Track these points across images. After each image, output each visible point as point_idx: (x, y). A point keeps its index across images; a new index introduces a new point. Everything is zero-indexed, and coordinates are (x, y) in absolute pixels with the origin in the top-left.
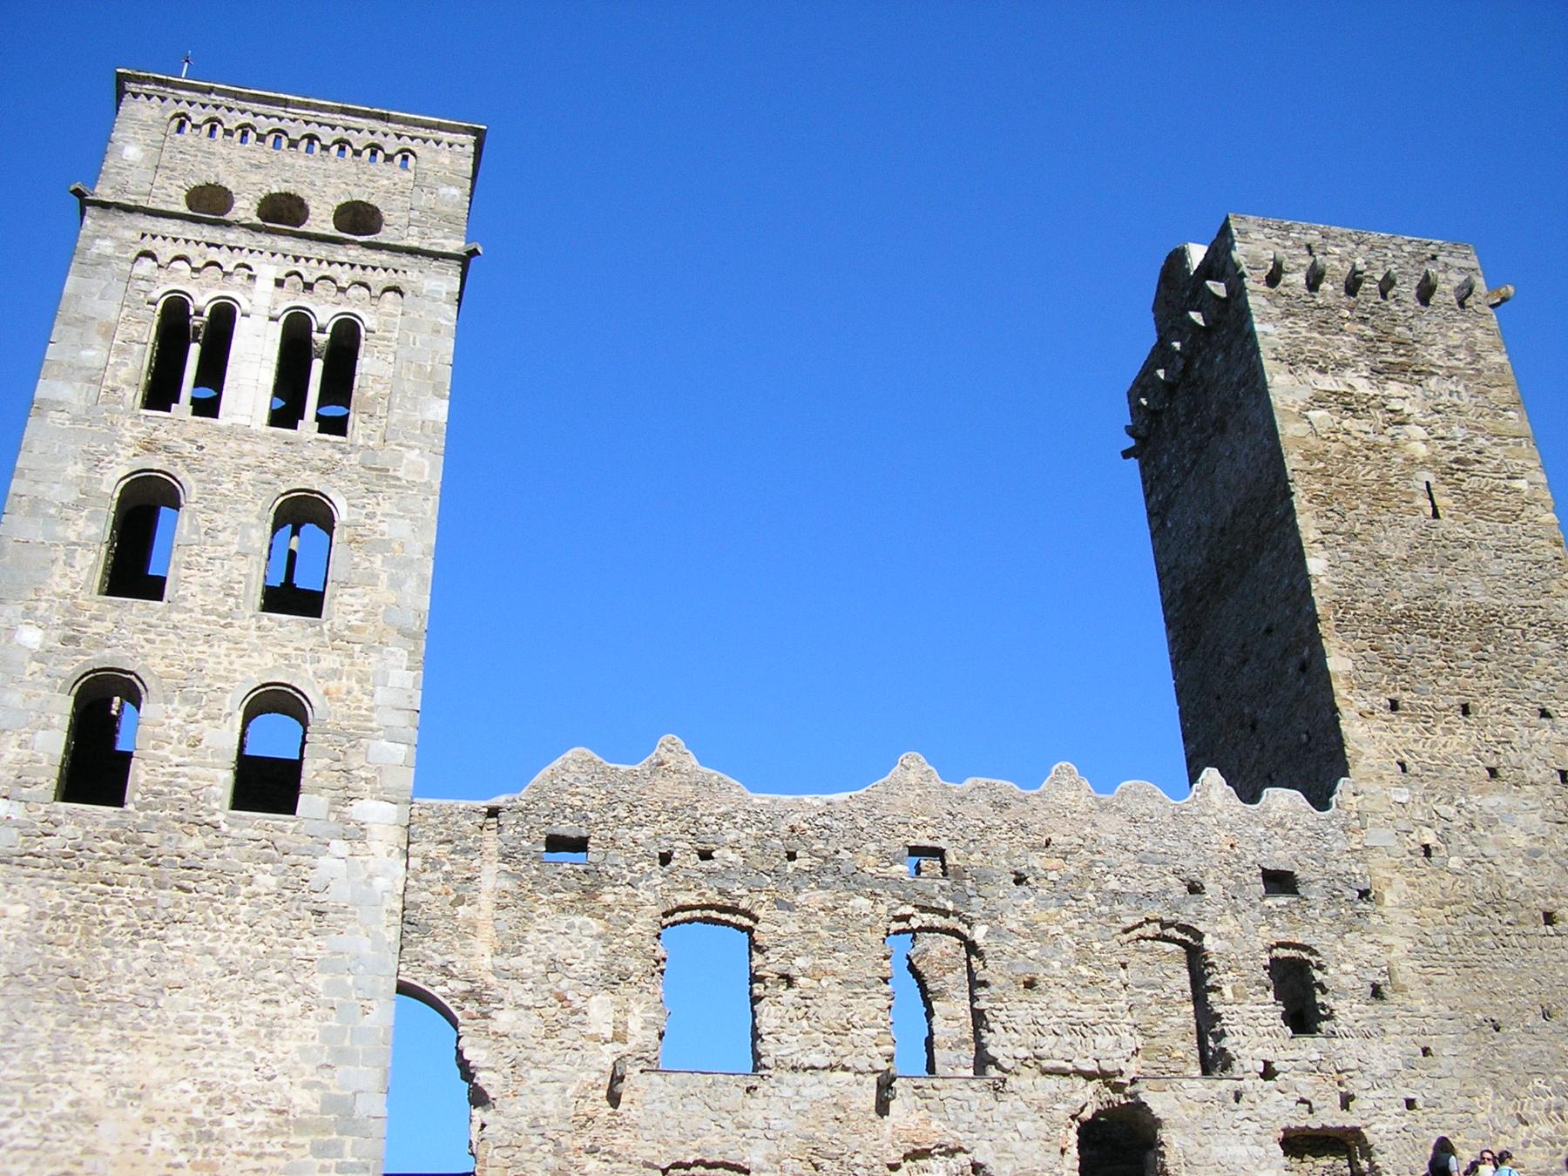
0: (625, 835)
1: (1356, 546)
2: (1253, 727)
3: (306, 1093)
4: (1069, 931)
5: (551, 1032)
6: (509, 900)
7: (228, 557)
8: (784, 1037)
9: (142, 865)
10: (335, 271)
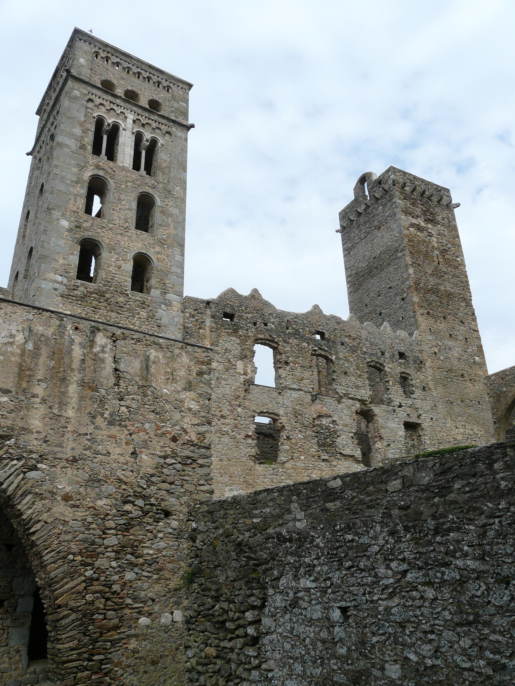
0: (245, 316)
1: (420, 268)
2: (380, 314)
4: (354, 360)
5: (227, 370)
6: (214, 330)
7: (125, 209)
8: (287, 379)
9: (105, 304)
10: (150, 122)
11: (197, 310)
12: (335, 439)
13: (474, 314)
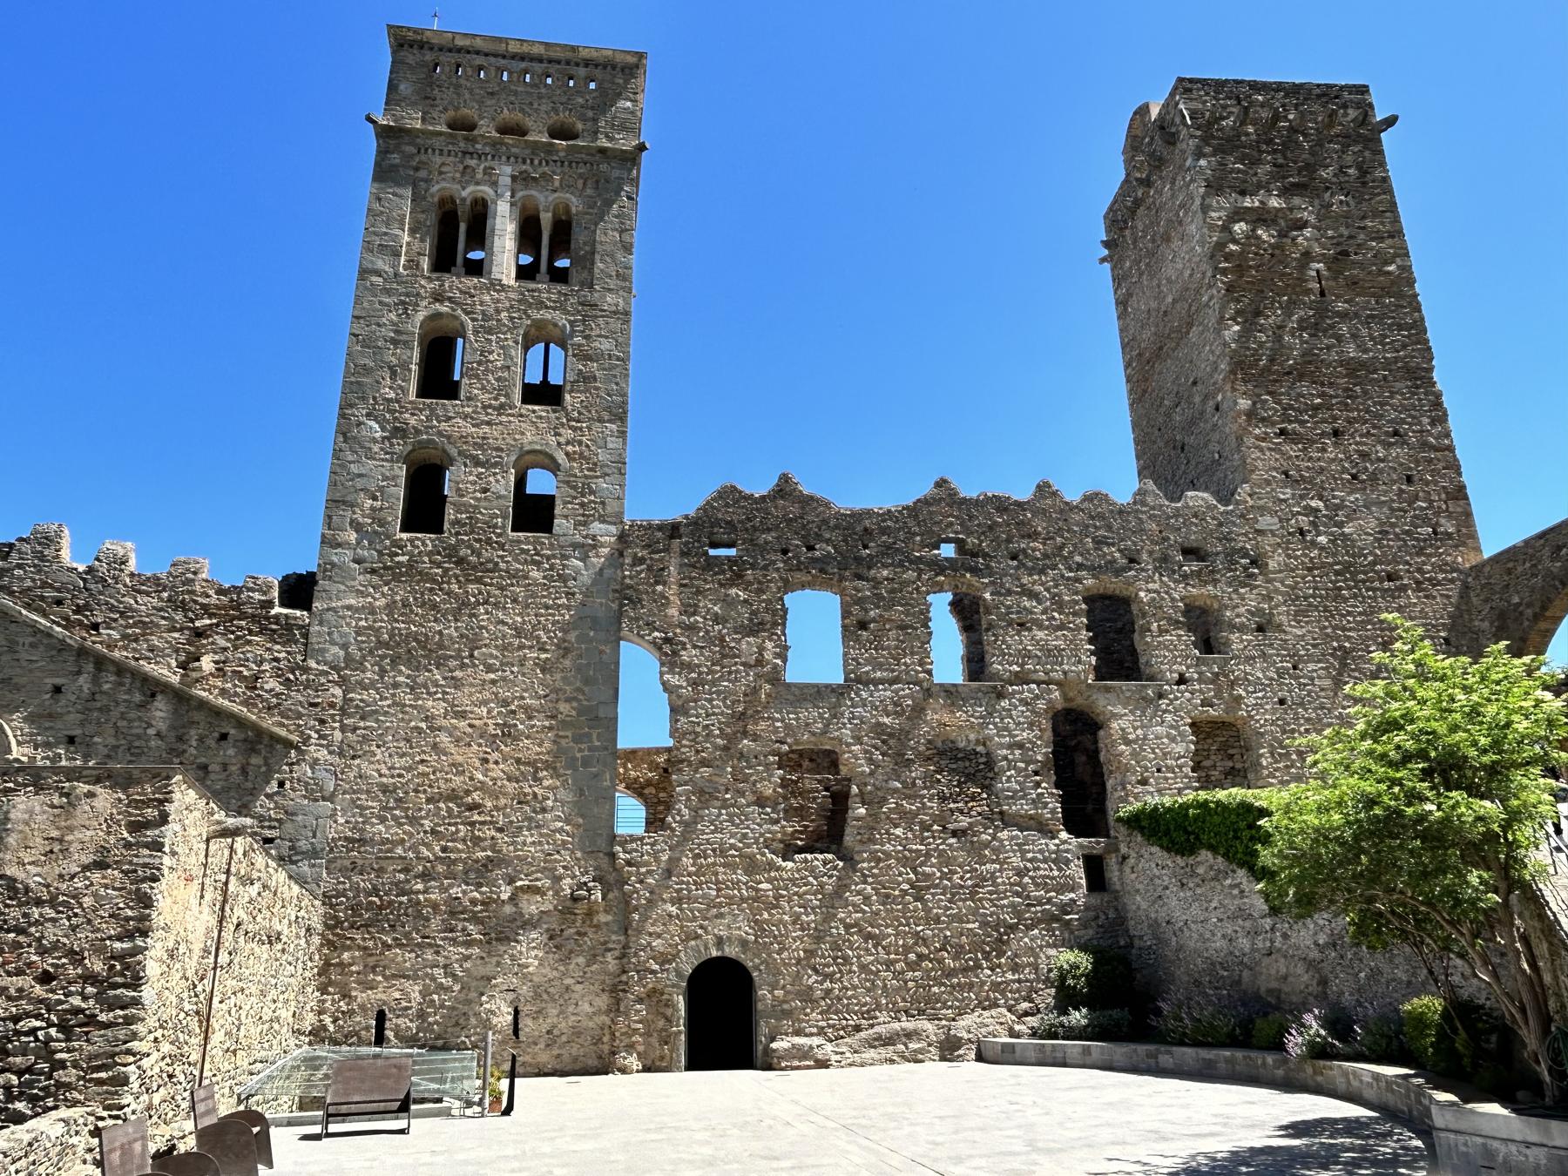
2: (1183, 449)
3: (568, 706)
11: (650, 546)
12: (987, 782)
13: (1437, 404)
